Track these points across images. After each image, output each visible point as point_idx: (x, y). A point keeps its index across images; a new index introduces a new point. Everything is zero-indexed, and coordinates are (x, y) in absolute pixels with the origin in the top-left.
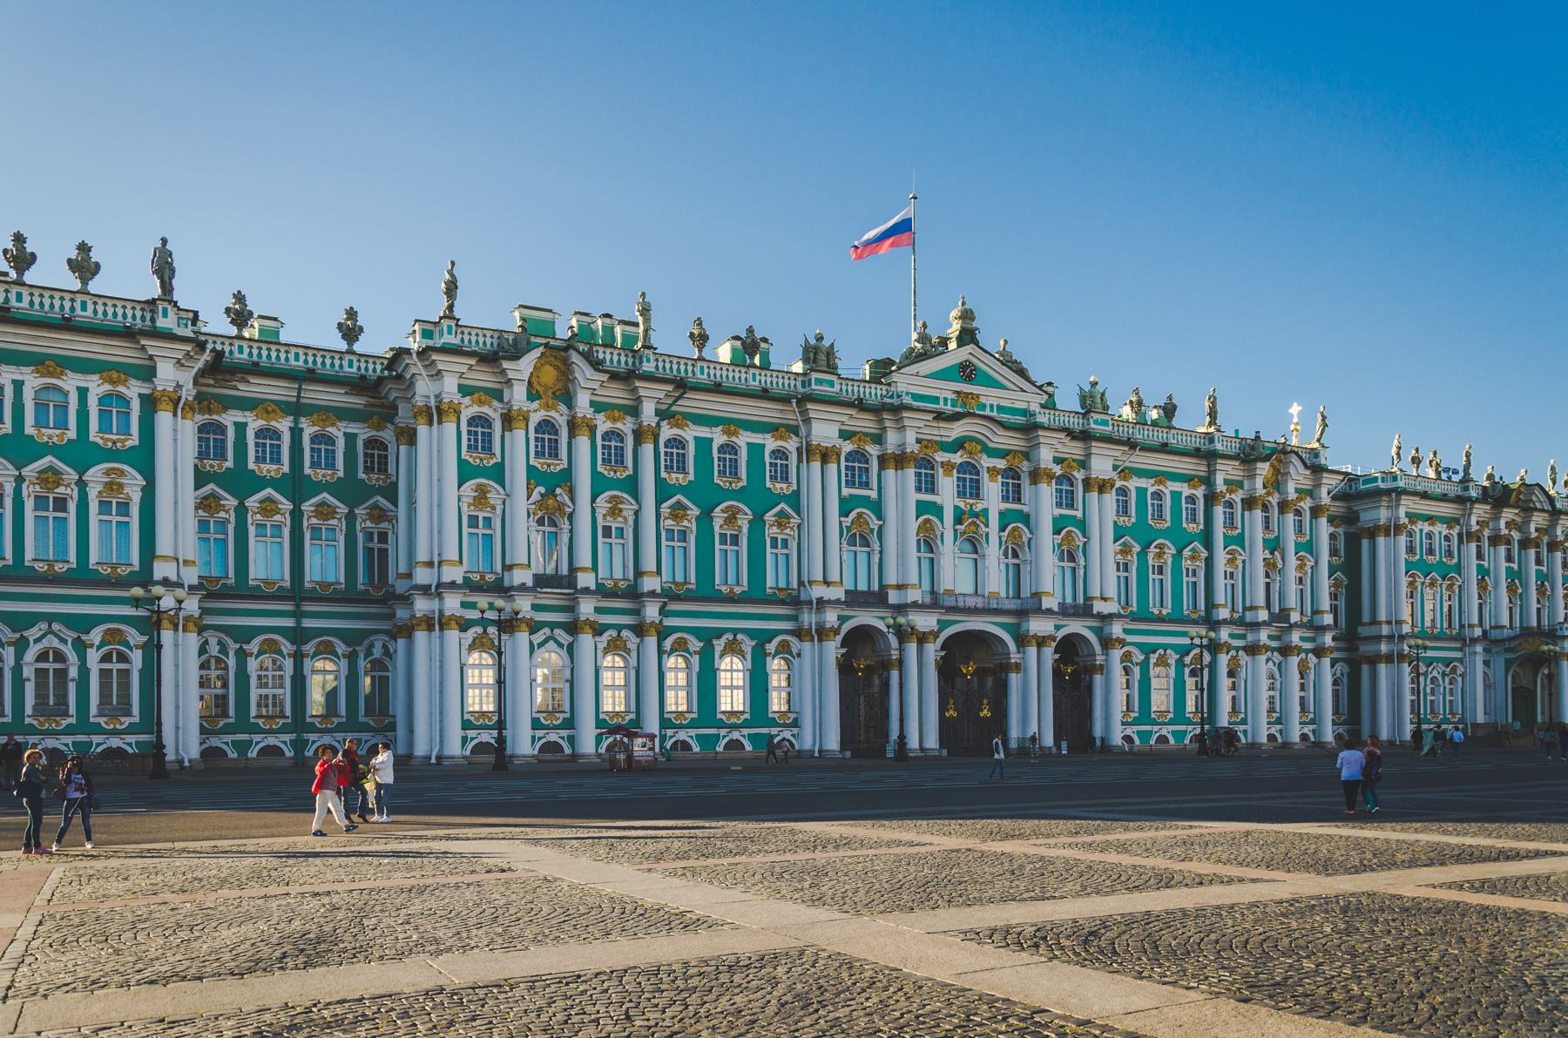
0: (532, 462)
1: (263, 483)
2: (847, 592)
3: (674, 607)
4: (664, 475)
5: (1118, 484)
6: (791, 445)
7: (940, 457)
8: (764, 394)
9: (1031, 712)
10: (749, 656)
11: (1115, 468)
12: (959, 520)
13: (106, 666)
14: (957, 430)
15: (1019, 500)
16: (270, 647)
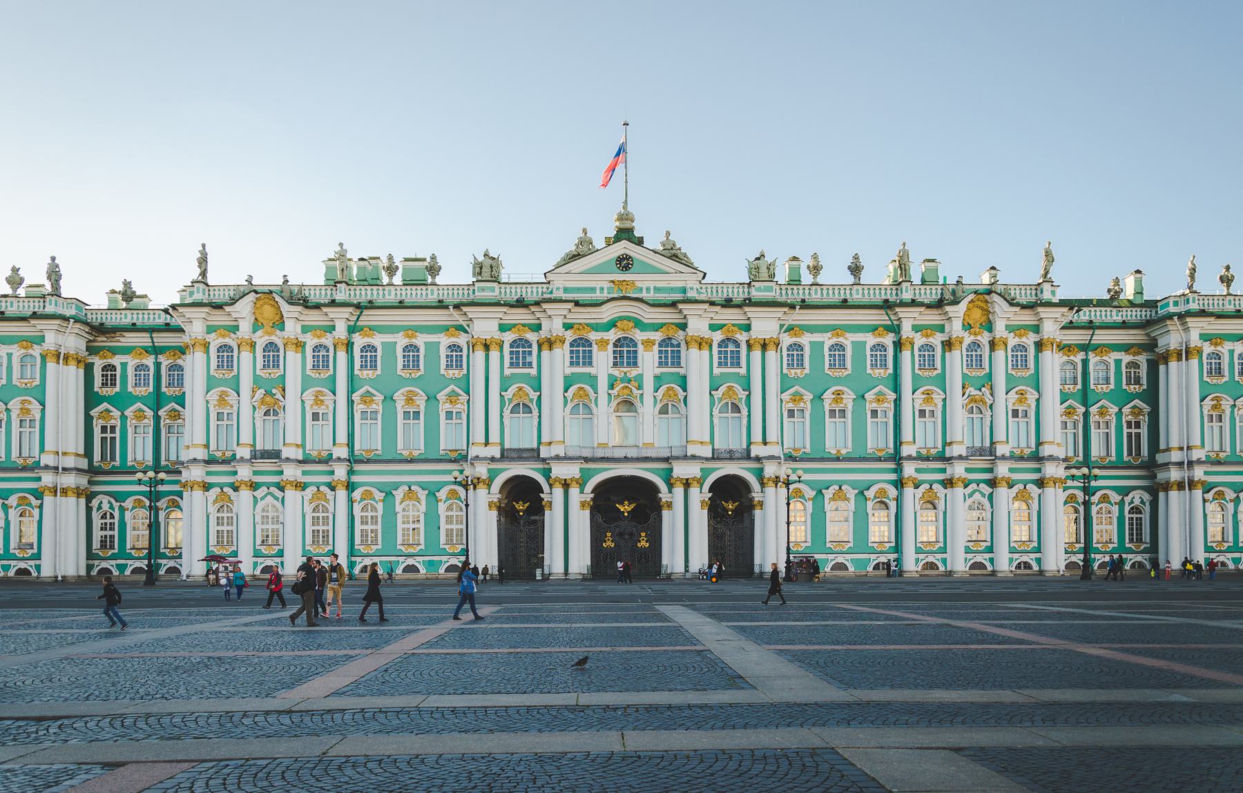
0: (258, 372)
1: (137, 399)
2: (503, 451)
3: (357, 467)
4: (356, 372)
5: (787, 340)
6: (462, 340)
7: (593, 336)
8: (441, 305)
9: (685, 542)
10: (424, 502)
11: (782, 326)
12: (612, 387)
13: (450, 513)
14: (607, 313)
15: (679, 365)
16: (139, 504)
